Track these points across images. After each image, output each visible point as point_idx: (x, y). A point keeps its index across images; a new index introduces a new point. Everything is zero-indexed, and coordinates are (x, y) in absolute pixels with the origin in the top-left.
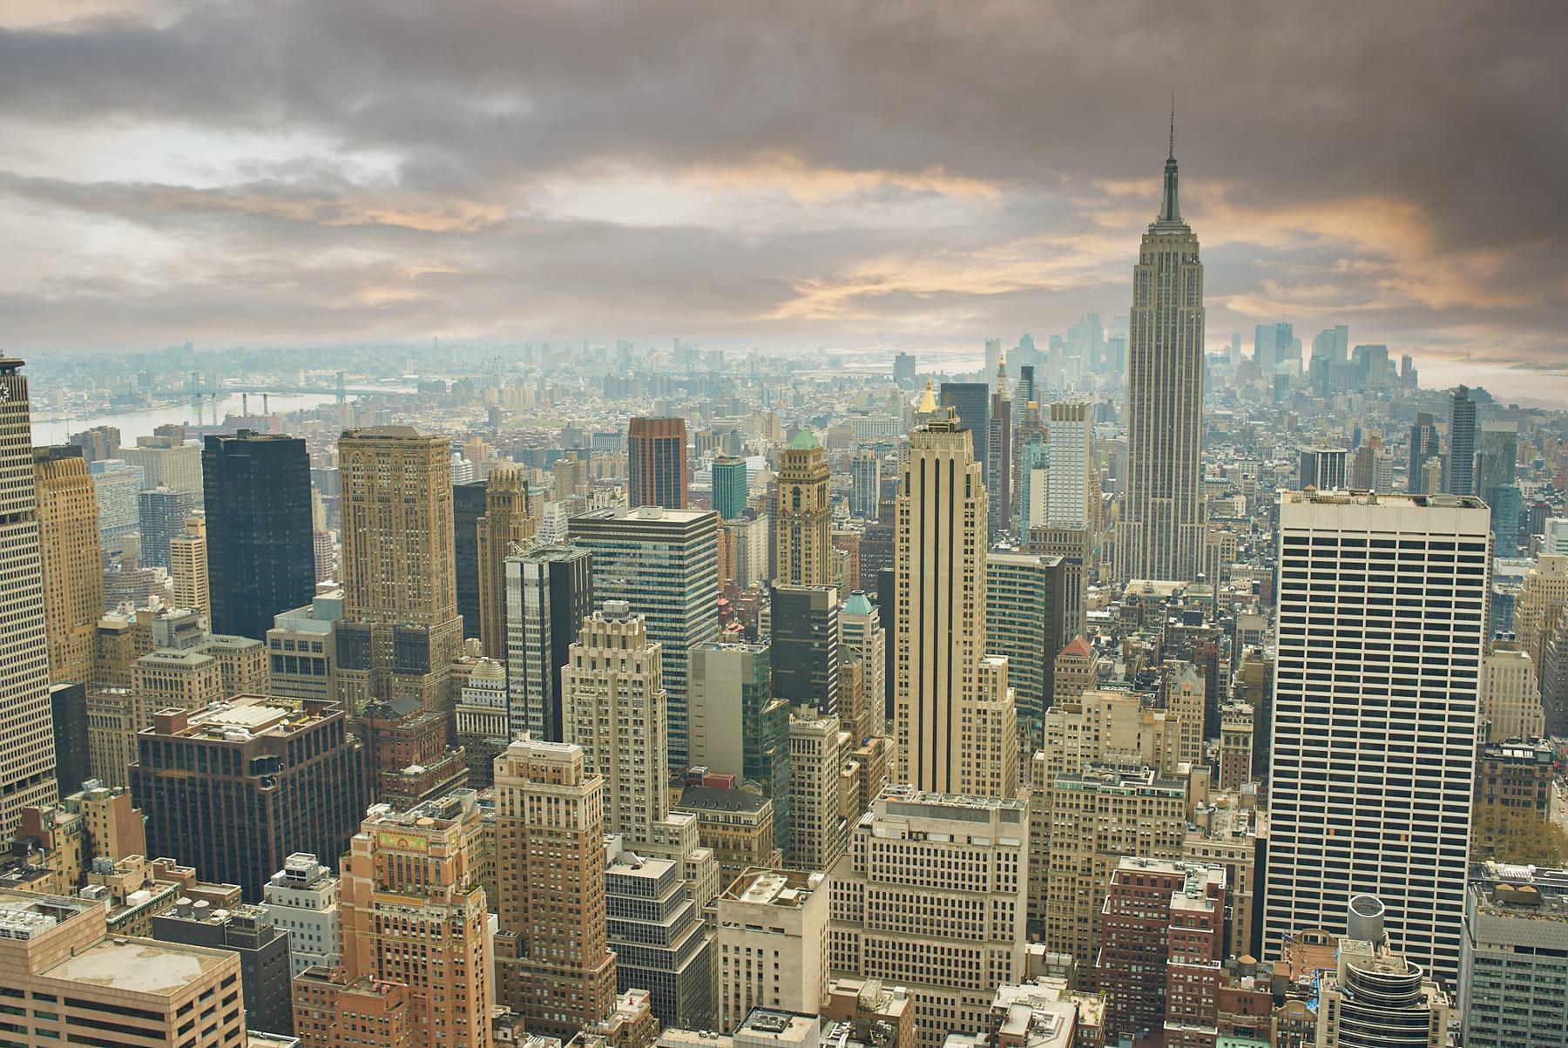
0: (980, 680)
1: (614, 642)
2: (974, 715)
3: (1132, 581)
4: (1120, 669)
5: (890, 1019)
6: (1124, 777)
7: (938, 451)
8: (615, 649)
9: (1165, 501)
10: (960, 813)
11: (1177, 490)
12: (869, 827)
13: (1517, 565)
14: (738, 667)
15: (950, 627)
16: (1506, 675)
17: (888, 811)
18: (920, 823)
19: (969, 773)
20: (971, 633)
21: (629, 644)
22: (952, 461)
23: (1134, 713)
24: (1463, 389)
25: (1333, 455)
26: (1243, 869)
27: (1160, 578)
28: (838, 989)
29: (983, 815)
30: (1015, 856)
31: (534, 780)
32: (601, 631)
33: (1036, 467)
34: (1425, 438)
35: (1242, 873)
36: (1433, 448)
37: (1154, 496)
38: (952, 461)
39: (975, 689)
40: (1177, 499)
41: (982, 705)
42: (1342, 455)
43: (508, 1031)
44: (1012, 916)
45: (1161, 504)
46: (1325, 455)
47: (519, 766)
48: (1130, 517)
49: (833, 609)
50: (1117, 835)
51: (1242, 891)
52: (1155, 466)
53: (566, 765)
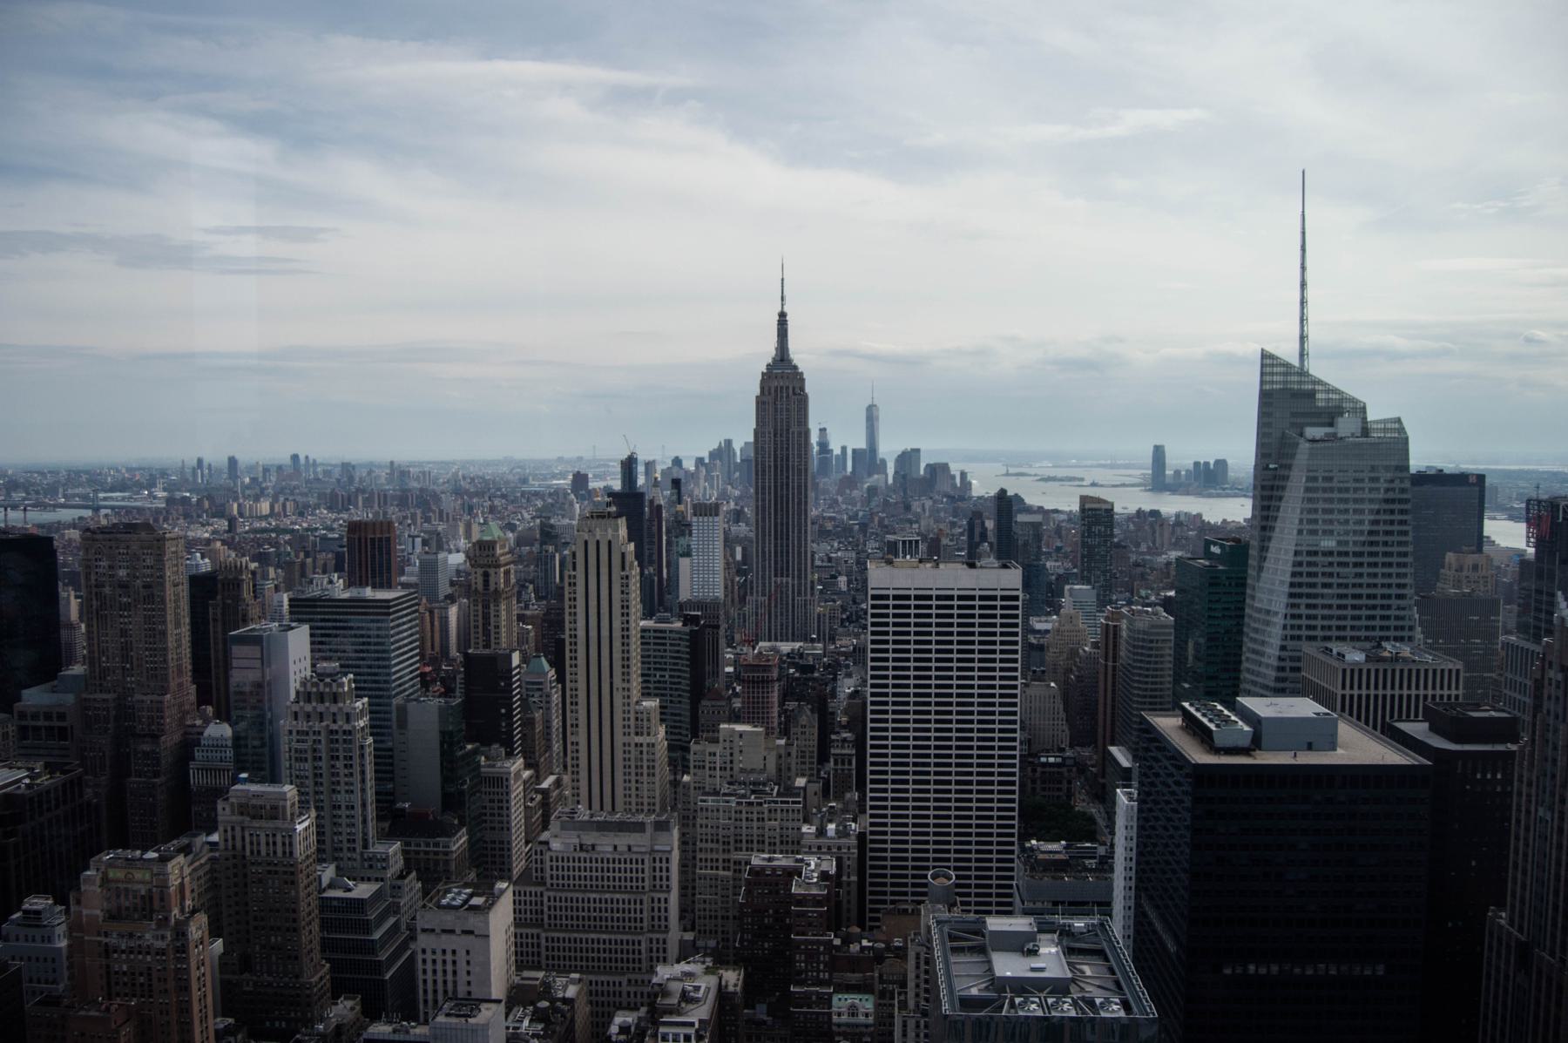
3: (761, 644)
9: (784, 580)
11: (793, 570)
13: (1046, 621)
24: (1003, 491)
25: (910, 542)
27: (781, 641)
33: (682, 556)
34: (977, 530)
36: (984, 536)
37: (776, 576)
40: (793, 577)
42: (917, 542)
45: (782, 583)
46: (904, 542)
48: (757, 592)
52: (776, 552)
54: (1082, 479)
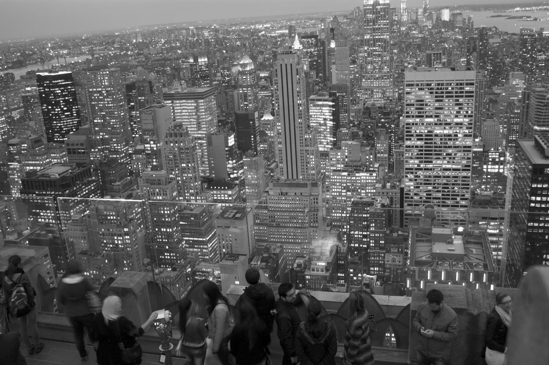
0: (306, 140)
1: (178, 135)
2: (304, 152)
4: (361, 133)
5: (274, 254)
6: (355, 170)
7: (286, 61)
8: (178, 138)
10: (298, 185)
12: (268, 192)
14: (224, 142)
15: (294, 122)
16: (490, 127)
17: (274, 186)
18: (285, 190)
19: (304, 172)
20: (302, 124)
21: (183, 135)
22: (291, 64)
23: (359, 147)
26: (396, 198)
28: (258, 246)
29: (305, 185)
30: (317, 198)
31: (152, 184)
32: (173, 132)
35: (395, 199)
38: (291, 64)
39: (304, 143)
41: (307, 148)
43: (150, 267)
44: (317, 218)
47: (147, 179)
49: (257, 118)
50: (354, 190)
51: (396, 205)
53: (162, 178)
54: (530, 17)
